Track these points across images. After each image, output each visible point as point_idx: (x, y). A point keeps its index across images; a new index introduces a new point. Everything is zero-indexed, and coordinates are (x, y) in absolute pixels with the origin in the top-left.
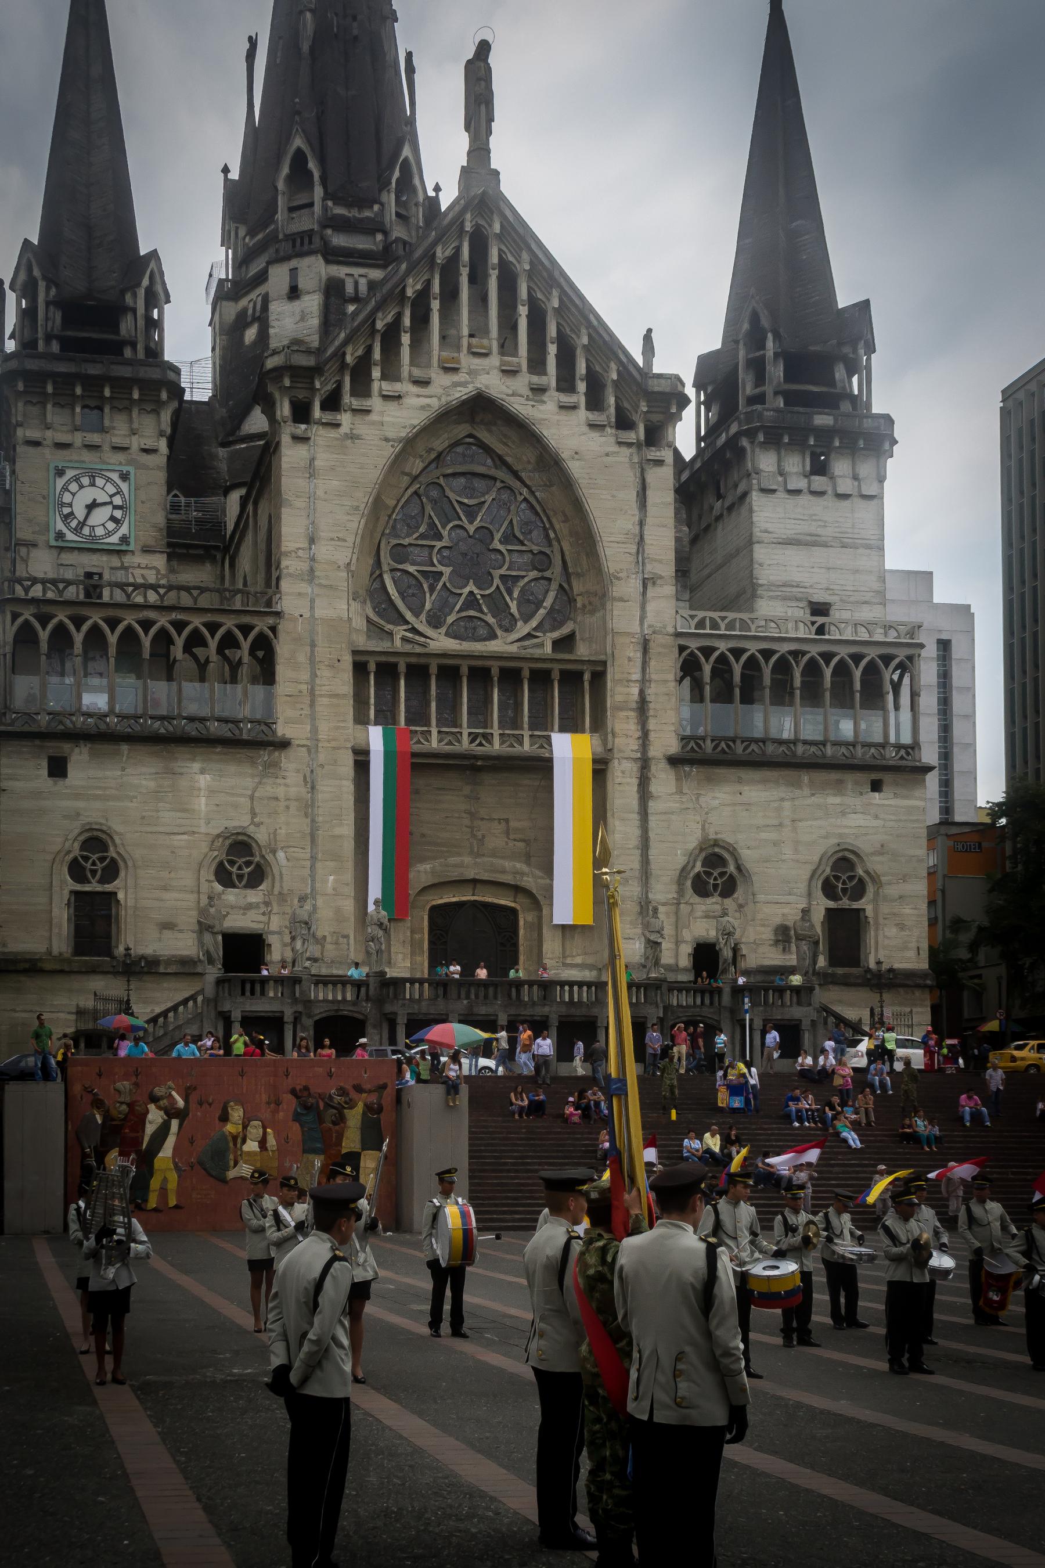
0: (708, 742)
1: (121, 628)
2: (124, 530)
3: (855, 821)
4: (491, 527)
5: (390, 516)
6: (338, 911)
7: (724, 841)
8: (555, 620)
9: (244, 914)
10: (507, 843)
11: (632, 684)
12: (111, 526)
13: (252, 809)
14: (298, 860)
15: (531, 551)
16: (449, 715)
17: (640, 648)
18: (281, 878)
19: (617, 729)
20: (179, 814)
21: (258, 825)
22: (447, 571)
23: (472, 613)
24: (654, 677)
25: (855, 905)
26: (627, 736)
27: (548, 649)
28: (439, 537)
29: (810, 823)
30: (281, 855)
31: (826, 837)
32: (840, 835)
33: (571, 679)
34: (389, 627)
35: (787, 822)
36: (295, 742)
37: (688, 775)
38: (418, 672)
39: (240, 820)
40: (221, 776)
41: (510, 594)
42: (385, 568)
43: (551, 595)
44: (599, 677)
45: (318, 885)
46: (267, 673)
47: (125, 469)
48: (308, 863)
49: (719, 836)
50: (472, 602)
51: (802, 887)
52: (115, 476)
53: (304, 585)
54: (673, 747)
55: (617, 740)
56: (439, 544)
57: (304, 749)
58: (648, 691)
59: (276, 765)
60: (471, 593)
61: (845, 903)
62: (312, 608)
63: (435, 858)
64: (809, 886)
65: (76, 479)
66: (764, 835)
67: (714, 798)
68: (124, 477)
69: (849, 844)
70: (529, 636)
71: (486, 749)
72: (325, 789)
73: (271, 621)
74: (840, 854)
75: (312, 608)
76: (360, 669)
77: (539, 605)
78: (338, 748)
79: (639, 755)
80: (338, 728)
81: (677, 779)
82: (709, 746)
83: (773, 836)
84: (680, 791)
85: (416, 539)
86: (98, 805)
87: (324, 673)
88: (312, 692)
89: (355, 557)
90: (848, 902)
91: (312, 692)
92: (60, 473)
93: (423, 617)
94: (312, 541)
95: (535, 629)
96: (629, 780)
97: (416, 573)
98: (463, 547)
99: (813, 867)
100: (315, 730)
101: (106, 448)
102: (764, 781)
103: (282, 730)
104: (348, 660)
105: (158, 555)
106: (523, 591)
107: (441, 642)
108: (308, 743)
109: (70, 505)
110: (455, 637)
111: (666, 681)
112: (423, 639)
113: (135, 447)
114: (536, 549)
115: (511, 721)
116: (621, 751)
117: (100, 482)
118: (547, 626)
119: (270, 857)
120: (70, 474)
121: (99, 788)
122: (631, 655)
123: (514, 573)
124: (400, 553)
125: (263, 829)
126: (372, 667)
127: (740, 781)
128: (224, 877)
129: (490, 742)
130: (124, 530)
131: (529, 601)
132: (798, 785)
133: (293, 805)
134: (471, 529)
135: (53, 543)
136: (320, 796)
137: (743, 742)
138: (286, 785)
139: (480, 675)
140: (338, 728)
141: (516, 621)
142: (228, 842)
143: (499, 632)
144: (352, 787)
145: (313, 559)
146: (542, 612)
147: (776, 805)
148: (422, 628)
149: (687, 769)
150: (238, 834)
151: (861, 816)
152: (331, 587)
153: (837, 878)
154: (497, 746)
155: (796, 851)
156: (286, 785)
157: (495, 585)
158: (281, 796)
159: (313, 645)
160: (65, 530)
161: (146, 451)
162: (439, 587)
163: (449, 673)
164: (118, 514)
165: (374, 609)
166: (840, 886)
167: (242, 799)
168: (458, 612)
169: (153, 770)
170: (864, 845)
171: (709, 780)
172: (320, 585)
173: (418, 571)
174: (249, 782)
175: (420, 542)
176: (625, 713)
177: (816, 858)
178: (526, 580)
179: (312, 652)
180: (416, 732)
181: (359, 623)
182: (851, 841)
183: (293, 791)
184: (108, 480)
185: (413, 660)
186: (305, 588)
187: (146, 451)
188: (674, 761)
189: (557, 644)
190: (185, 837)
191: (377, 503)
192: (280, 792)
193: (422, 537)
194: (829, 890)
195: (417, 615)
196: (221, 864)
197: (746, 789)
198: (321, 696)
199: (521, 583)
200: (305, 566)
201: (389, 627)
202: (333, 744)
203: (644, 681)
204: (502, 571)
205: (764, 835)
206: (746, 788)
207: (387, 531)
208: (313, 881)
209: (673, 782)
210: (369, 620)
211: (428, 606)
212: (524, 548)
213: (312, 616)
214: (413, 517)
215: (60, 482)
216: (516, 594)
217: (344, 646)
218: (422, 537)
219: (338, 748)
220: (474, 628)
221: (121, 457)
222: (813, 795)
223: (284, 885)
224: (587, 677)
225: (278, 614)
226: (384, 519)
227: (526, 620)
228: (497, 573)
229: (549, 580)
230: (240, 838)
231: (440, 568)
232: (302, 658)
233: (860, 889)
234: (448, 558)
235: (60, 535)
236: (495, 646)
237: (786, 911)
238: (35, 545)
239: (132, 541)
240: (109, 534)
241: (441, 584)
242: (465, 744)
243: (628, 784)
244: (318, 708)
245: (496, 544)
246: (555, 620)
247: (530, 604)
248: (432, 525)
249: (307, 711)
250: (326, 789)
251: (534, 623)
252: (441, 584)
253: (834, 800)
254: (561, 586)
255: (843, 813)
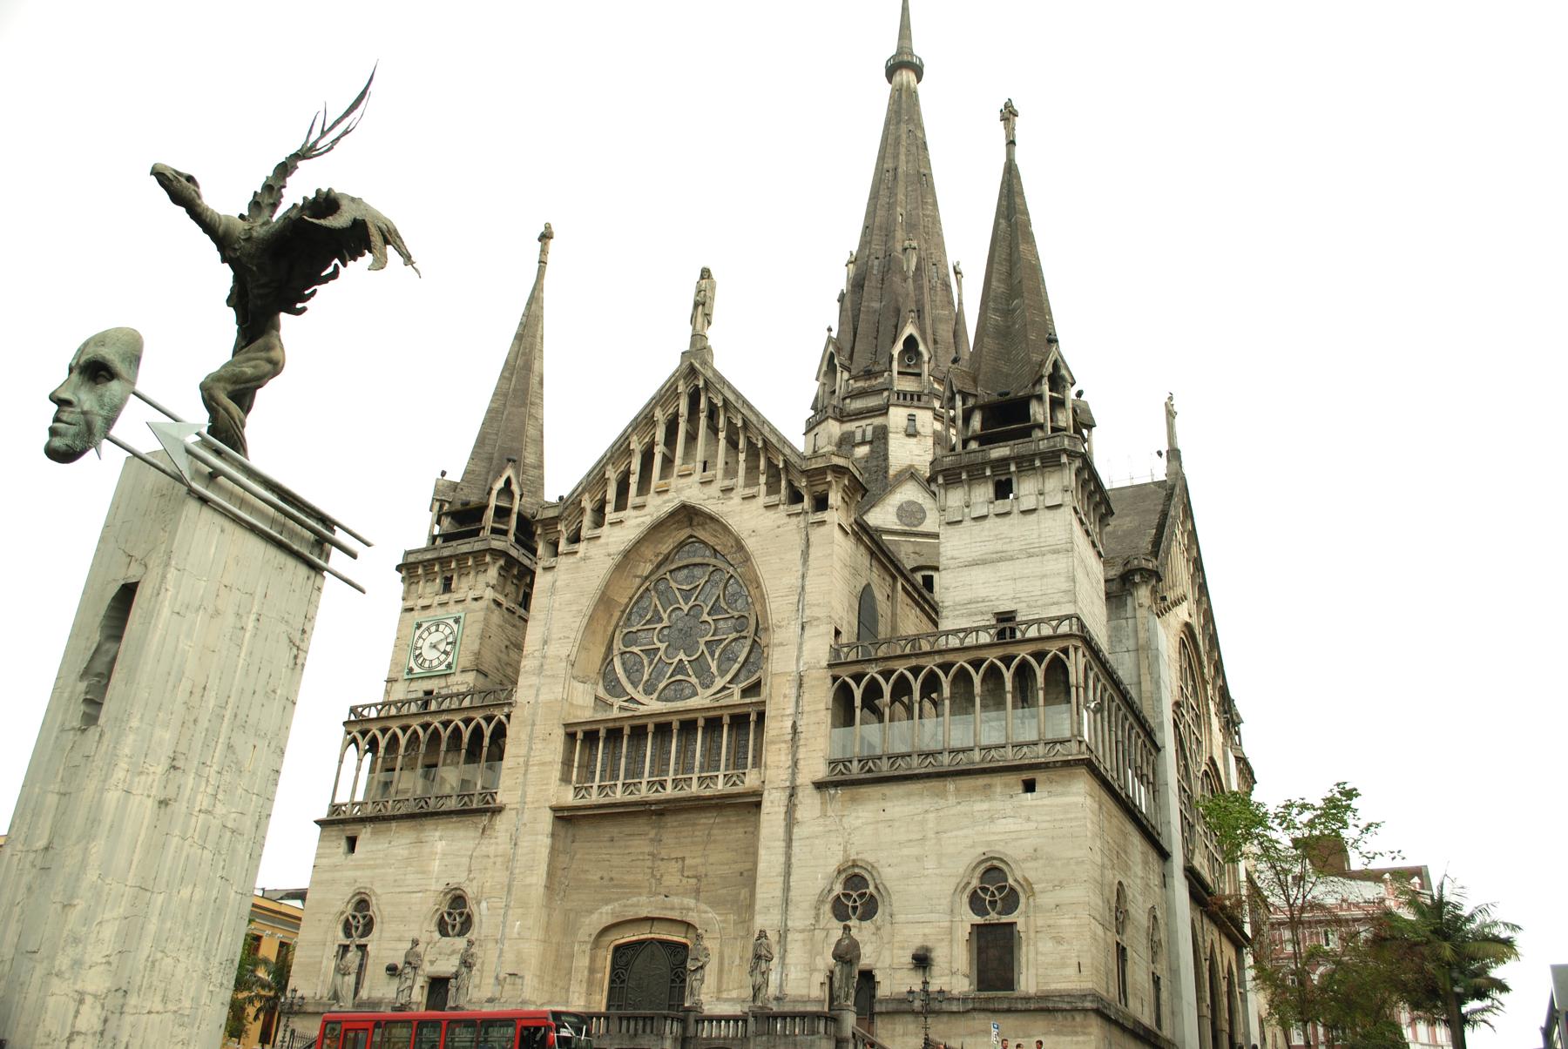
0: (855, 763)
1: (409, 733)
2: (450, 659)
3: (1010, 825)
4: (702, 604)
5: (623, 612)
6: (519, 953)
7: (862, 860)
8: (749, 671)
9: (448, 960)
10: (681, 881)
11: (786, 718)
12: (443, 656)
13: (470, 866)
14: (495, 908)
15: (733, 617)
16: (634, 771)
17: (795, 684)
18: (481, 927)
19: (768, 763)
20: (420, 876)
21: (471, 881)
22: (663, 646)
23: (679, 677)
24: (806, 708)
25: (1005, 919)
26: (778, 767)
27: (737, 698)
28: (661, 620)
29: (955, 833)
30: (484, 905)
31: (973, 846)
32: (988, 843)
33: (739, 722)
34: (610, 700)
35: (931, 834)
36: (508, 807)
37: (833, 798)
38: (614, 735)
39: (459, 878)
40: (453, 840)
41: (712, 655)
42: (616, 652)
43: (746, 650)
44: (761, 716)
45: (507, 930)
46: (497, 754)
47: (457, 615)
48: (502, 911)
49: (860, 857)
50: (680, 668)
51: (945, 903)
52: (451, 622)
53: (534, 678)
54: (821, 772)
55: (768, 772)
56: (659, 626)
57: (514, 812)
58: (798, 723)
59: (492, 827)
60: (681, 660)
61: (993, 917)
62: (537, 695)
63: (617, 900)
64: (952, 903)
65: (428, 629)
66: (906, 851)
67: (858, 817)
68: (457, 621)
69: (999, 852)
70: (724, 688)
71: (663, 795)
72: (525, 844)
73: (506, 710)
74: (989, 864)
75: (537, 695)
76: (571, 737)
77: (735, 661)
78: (539, 808)
79: (788, 784)
80: (541, 790)
81: (822, 803)
82: (855, 766)
83: (915, 851)
84: (824, 815)
85: (645, 624)
86: (368, 873)
87: (538, 746)
88: (527, 764)
89: (575, 649)
90: (996, 916)
91: (527, 764)
92: (419, 626)
93: (640, 688)
94: (545, 642)
95: (729, 682)
96: (777, 809)
97: (639, 653)
98: (680, 625)
99: (958, 880)
100: (524, 795)
101: (452, 602)
102: (909, 795)
103: (501, 798)
104: (559, 734)
105: (471, 673)
106: (724, 650)
107: (652, 705)
108: (518, 806)
109: (421, 648)
110: (667, 700)
111: (816, 711)
112: (636, 706)
113: (469, 599)
114: (736, 614)
115: (685, 765)
116: (770, 782)
117: (442, 627)
118: (742, 676)
119: (474, 908)
120: (425, 626)
121: (372, 859)
122: (787, 692)
123: (716, 638)
124: (630, 639)
125: (475, 882)
126: (580, 736)
127: (884, 797)
128: (443, 929)
129: (664, 789)
130: (450, 659)
131: (729, 659)
132: (943, 794)
133: (499, 860)
134: (686, 608)
135: (406, 677)
136: (520, 851)
137: (889, 758)
138: (497, 844)
139: (663, 730)
140: (541, 790)
141: (714, 676)
142: (449, 896)
143: (699, 689)
144: (548, 841)
145: (544, 657)
146: (736, 666)
147: (920, 817)
148: (636, 697)
149: (832, 792)
150: (456, 889)
151: (1011, 820)
152: (553, 676)
153: (984, 890)
154: (669, 792)
155: (940, 865)
156: (497, 844)
157: (700, 651)
158: (492, 854)
159: (533, 724)
160: (415, 667)
161: (476, 599)
162: (655, 661)
163: (639, 732)
164: (448, 648)
165: (606, 689)
166: (988, 898)
167: (464, 859)
168: (670, 677)
169: (408, 841)
170: (1012, 851)
171: (853, 800)
172: (547, 676)
173: (642, 651)
174: (471, 844)
175: (645, 627)
176: (777, 746)
177: (961, 871)
178: (727, 641)
179: (532, 730)
180: (606, 786)
181: (590, 701)
182: (999, 849)
183: (501, 849)
184: (447, 625)
185: (611, 725)
186: (534, 680)
187: (476, 599)
188: (820, 786)
189: (745, 692)
190: (420, 894)
191: (604, 601)
192: (491, 850)
193: (648, 622)
194: (976, 903)
195: (636, 687)
196: (442, 917)
197: (888, 805)
198: (533, 765)
199: (722, 646)
200: (537, 663)
201: (610, 700)
202: (536, 805)
203: (798, 712)
204: (707, 638)
205: (906, 851)
206: (889, 804)
207: (621, 624)
208: (504, 927)
209: (818, 806)
210: (596, 698)
211: (645, 677)
212: (727, 616)
213: (536, 702)
214: (644, 609)
215: (418, 632)
216: (716, 657)
217: (555, 722)
218: (648, 622)
219: (539, 808)
220: (682, 690)
221: (460, 606)
222: (959, 803)
223: (482, 931)
224: (753, 717)
225: (510, 704)
226: (617, 614)
227: (723, 673)
228: (702, 641)
229: (745, 637)
230: (458, 892)
231: (659, 645)
232: (524, 737)
233: (1011, 901)
234: (668, 635)
235: (411, 670)
236: (694, 703)
237: (927, 931)
238: (396, 681)
239: (454, 666)
240: (440, 664)
241: (658, 657)
242: (644, 793)
243: (776, 813)
244: (529, 776)
245: (705, 617)
246: (749, 671)
247: (727, 658)
248: (656, 611)
249: (521, 777)
250: (525, 843)
251: (728, 677)
252: (658, 657)
253: (981, 806)
254: (755, 641)
255: (992, 819)
